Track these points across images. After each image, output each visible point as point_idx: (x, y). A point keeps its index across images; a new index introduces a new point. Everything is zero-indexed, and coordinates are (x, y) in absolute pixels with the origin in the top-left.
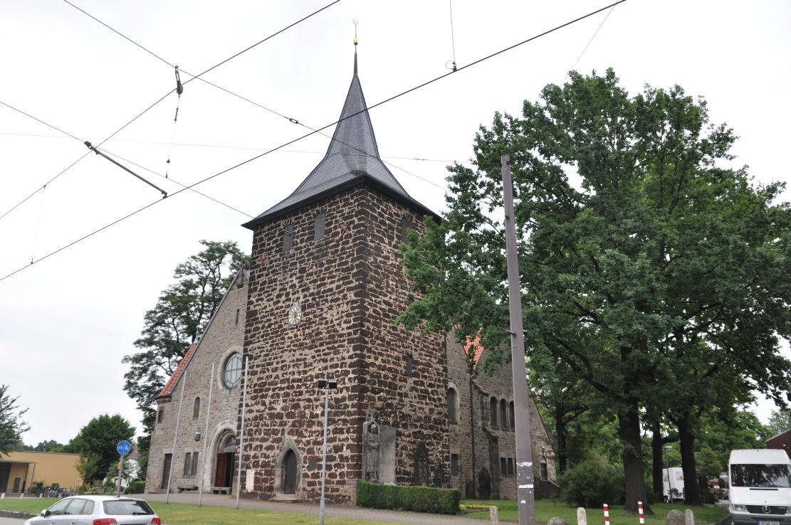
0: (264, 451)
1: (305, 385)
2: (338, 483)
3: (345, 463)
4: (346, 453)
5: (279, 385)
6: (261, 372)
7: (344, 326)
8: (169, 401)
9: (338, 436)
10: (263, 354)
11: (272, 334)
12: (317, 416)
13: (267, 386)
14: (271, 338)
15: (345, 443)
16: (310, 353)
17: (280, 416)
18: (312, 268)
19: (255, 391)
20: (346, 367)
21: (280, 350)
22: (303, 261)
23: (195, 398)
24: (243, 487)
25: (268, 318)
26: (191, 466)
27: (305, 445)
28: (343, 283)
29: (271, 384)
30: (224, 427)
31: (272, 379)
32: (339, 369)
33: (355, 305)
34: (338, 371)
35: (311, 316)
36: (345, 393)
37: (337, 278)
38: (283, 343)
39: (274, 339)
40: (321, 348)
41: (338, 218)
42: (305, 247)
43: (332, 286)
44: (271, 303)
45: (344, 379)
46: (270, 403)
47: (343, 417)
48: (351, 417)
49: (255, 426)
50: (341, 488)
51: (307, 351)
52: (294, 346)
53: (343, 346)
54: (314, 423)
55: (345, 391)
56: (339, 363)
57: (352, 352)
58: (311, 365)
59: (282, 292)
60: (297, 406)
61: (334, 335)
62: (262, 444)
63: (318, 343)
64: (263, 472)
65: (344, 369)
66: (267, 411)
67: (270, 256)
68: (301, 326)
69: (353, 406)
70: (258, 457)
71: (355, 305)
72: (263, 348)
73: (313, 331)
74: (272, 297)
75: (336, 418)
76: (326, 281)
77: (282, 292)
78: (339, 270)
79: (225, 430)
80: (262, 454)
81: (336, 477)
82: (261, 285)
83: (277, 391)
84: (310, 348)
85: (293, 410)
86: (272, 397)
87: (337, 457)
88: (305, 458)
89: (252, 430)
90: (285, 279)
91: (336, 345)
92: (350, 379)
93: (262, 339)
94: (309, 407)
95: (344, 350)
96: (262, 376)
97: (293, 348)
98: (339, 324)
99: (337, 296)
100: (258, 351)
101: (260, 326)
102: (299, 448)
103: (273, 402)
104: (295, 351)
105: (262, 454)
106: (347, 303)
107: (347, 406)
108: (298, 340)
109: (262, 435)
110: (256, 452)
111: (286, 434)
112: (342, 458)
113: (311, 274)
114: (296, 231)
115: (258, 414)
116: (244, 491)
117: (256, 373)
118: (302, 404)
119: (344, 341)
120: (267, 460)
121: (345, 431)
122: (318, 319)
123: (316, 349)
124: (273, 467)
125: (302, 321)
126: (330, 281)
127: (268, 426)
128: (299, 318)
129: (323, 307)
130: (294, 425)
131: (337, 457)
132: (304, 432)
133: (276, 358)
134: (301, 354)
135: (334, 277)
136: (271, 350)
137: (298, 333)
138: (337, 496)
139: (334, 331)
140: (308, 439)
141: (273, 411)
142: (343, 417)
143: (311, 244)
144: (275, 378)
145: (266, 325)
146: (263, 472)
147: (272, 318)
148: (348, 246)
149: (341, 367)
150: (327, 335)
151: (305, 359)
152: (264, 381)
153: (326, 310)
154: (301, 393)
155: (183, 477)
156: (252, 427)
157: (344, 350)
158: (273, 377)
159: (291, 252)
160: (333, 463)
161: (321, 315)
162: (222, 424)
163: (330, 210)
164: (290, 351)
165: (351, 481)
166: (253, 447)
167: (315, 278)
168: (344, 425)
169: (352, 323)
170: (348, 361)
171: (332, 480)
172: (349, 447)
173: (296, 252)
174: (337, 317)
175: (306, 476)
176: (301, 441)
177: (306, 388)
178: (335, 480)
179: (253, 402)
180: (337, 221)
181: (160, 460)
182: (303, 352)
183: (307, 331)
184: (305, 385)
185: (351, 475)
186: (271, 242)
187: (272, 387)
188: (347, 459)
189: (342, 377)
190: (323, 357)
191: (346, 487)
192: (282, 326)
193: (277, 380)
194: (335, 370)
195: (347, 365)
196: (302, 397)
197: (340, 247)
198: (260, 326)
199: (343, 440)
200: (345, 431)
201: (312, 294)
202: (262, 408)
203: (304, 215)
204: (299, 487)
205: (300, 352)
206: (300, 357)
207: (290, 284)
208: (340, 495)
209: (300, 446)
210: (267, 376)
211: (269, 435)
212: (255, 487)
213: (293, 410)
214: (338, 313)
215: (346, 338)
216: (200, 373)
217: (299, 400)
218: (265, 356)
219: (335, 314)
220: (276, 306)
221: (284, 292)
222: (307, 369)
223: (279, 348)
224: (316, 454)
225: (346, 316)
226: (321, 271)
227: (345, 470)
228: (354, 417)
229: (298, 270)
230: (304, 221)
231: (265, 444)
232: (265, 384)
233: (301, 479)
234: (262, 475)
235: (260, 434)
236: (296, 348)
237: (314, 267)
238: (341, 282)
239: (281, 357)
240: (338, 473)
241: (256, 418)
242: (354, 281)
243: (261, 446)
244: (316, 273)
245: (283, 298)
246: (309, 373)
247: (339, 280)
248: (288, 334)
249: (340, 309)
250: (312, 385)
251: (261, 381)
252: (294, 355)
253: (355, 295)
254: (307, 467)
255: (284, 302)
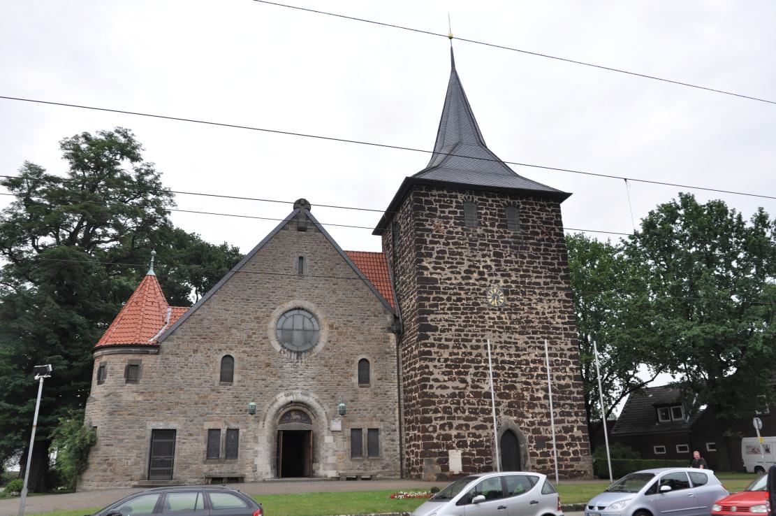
0: (474, 431)
1: (520, 368)
2: (572, 460)
3: (578, 443)
4: (577, 433)
5: (483, 364)
6: (454, 347)
7: (559, 321)
8: (157, 354)
9: (566, 418)
10: (453, 328)
11: (464, 309)
12: (539, 398)
13: (465, 363)
14: (462, 313)
15: (575, 425)
16: (521, 340)
17: (488, 395)
18: (510, 256)
19: (447, 366)
20: (565, 357)
21: (480, 329)
22: (499, 246)
23: (219, 359)
24: (446, 468)
25: (455, 291)
26: (224, 445)
27: (528, 425)
28: (551, 282)
29: (472, 361)
30: (290, 398)
31: (473, 357)
32: (558, 358)
33: (567, 304)
34: (558, 360)
35: (518, 303)
36: (567, 381)
37: (543, 275)
38: (483, 322)
39: (469, 315)
40: (535, 336)
41: (535, 219)
42: (497, 232)
43: (538, 280)
44: (458, 276)
45: (565, 368)
46: (473, 381)
47: (569, 402)
48: (578, 403)
49: (454, 403)
50: (575, 464)
51: (517, 336)
52: (499, 327)
53: (560, 339)
54: (536, 405)
55: (567, 379)
56: (559, 353)
57: (570, 346)
58: (525, 350)
59: (473, 269)
60: (513, 388)
61: (547, 329)
62: (468, 423)
63: (530, 331)
64: (475, 452)
65: (564, 359)
66: (469, 389)
67: (448, 226)
68: (505, 310)
69: (578, 393)
70: (464, 437)
71: (567, 304)
72: (454, 322)
73: (521, 318)
74: (458, 270)
75: (562, 402)
76: (531, 273)
77: (473, 269)
78: (545, 268)
79: (291, 402)
80: (469, 434)
81: (569, 455)
82: (438, 252)
83: (481, 370)
84: (521, 333)
85: (507, 391)
86: (475, 375)
87: (568, 437)
88: (531, 438)
89: (450, 407)
90: (475, 256)
91: (552, 336)
92: (571, 369)
93: (449, 312)
94: (527, 390)
95: (562, 343)
96: (456, 351)
97: (497, 329)
98: (553, 318)
99: (545, 291)
100: (443, 323)
101: (445, 297)
102: (522, 428)
103: (478, 381)
104: (500, 332)
105: (469, 434)
106: (559, 301)
107: (571, 393)
108: (503, 323)
109: (467, 413)
110: (459, 431)
111: (501, 414)
112: (573, 438)
113: (511, 262)
114: (483, 212)
115: (457, 391)
116: (448, 474)
117: (447, 347)
118: (518, 386)
119: (561, 334)
120: (478, 440)
121: (573, 414)
122: (526, 308)
123: (528, 336)
124: (487, 447)
125: (506, 305)
126: (535, 275)
127: (474, 404)
128: (501, 301)
129: (531, 297)
130: (510, 405)
131: (568, 437)
132: (525, 413)
133: (476, 336)
134: (510, 338)
135: (541, 273)
136: (465, 326)
137: (503, 316)
138: (572, 471)
139: (547, 322)
140: (531, 420)
141: (479, 390)
142: (569, 402)
143: (505, 233)
144: (477, 356)
145: (454, 298)
146: (475, 452)
147: (462, 292)
148: (552, 249)
149: (561, 357)
150: (541, 325)
151: (517, 343)
152: (460, 357)
153: (534, 301)
154: (516, 376)
155: (205, 462)
156: (448, 405)
157: (562, 343)
158: (474, 355)
159: (479, 231)
160: (564, 443)
161: (530, 304)
162: (287, 395)
163: (524, 208)
164: (494, 332)
165: (585, 458)
166: (455, 426)
167: (516, 266)
168: (571, 408)
169: (567, 320)
170: (569, 353)
171: (565, 457)
172: (579, 428)
173: (486, 234)
174: (550, 310)
175: (533, 454)
176: (522, 422)
177: (522, 371)
178: (568, 458)
179: (446, 378)
180: (534, 222)
181: (138, 437)
182: (513, 336)
183: (514, 316)
184: (520, 368)
185: (585, 452)
186: (447, 210)
187: (473, 365)
188: (579, 439)
189: (563, 366)
190: (538, 345)
191: (581, 463)
192: (478, 304)
193: (479, 358)
194: (555, 359)
195: (568, 356)
196: (518, 380)
197: (542, 247)
198: (445, 297)
199: (572, 422)
200: (573, 414)
201: (513, 282)
202: (463, 385)
203: (490, 199)
204: (527, 465)
205: (508, 335)
206: (508, 340)
207: (483, 264)
208: (575, 471)
209: (522, 426)
210: (464, 353)
211: (477, 414)
212: (463, 468)
213: (507, 391)
214: (549, 307)
215: (563, 332)
216: (229, 323)
217: (515, 382)
218: (456, 330)
219: (546, 307)
220: (467, 281)
221: (477, 270)
222: (521, 353)
223: (477, 326)
224: (544, 434)
225: (560, 312)
226: (523, 263)
227: (579, 448)
228: (580, 402)
229: (492, 253)
230: (492, 205)
231: (472, 424)
232: (462, 360)
233: (529, 457)
234: (473, 455)
235: (464, 412)
236: (502, 330)
237: (513, 257)
238: (549, 280)
239: (483, 336)
240: (571, 451)
241: (453, 395)
242: (563, 282)
243: (467, 426)
244: (517, 263)
245: (475, 275)
246: (523, 357)
247: (546, 277)
248: (488, 314)
249: (552, 304)
250: (528, 369)
251: (454, 357)
252: (500, 337)
253: (566, 295)
254: (534, 447)
255: (477, 280)
